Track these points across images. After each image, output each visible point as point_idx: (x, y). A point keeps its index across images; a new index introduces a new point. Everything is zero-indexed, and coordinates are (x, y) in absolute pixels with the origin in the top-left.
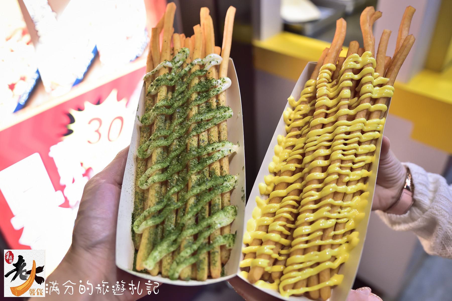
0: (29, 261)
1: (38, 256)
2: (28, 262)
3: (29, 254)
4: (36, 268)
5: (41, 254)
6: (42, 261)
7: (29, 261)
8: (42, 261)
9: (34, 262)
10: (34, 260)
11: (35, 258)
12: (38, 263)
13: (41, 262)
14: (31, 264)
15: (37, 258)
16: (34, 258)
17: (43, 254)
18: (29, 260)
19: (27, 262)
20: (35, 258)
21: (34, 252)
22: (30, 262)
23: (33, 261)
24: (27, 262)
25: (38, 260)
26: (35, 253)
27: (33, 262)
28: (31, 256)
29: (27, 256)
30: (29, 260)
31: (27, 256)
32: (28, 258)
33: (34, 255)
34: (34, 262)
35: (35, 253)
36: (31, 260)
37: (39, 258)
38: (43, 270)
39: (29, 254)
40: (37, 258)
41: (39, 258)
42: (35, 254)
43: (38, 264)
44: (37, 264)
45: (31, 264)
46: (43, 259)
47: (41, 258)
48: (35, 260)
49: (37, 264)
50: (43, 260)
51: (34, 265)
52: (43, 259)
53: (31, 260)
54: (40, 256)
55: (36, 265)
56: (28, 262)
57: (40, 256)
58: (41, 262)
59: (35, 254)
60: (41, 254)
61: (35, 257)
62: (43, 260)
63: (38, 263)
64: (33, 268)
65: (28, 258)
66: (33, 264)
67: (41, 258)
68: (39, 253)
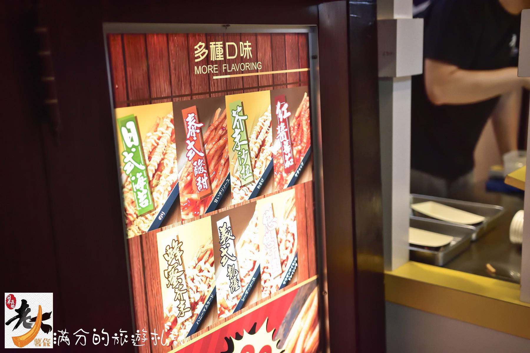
0: (34, 307)
1: (45, 300)
2: (32, 308)
3: (34, 298)
4: (42, 314)
5: (49, 297)
6: (50, 306)
7: (34, 307)
8: (50, 306)
9: (40, 307)
10: (40, 305)
11: (41, 302)
12: (45, 308)
13: (48, 308)
14: (37, 310)
15: (44, 302)
16: (39, 303)
17: (50, 298)
18: (34, 305)
19: (32, 307)
20: (41, 302)
21: (40, 296)
22: (35, 307)
23: (38, 306)
24: (32, 307)
25: (45, 305)
26: (41, 296)
27: (38, 308)
28: (37, 300)
29: (32, 301)
30: (34, 305)
31: (32, 301)
32: (32, 302)
33: (40, 299)
34: (40, 307)
35: (41, 296)
36: (37, 305)
37: (46, 303)
38: (51, 316)
39: (34, 298)
40: (44, 302)
41: (46, 303)
42: (41, 297)
43: (45, 310)
44: (43, 309)
45: (37, 310)
46: (50, 304)
47: (49, 302)
48: (41, 305)
49: (43, 309)
50: (50, 305)
51: (40, 311)
52: (50, 304)
53: (37, 305)
54: (47, 300)
55: (42, 311)
56: (32, 308)
57: (47, 300)
58: (49, 308)
59: (41, 297)
60: (49, 297)
61: (41, 302)
62: (50, 305)
63: (45, 308)
64: (39, 314)
65: (32, 302)
66: (38, 309)
67: (49, 302)
68: (46, 297)
